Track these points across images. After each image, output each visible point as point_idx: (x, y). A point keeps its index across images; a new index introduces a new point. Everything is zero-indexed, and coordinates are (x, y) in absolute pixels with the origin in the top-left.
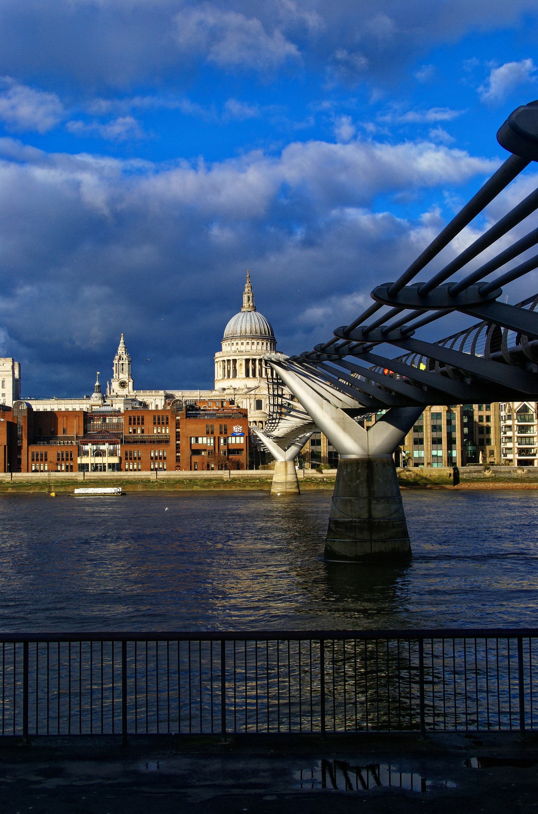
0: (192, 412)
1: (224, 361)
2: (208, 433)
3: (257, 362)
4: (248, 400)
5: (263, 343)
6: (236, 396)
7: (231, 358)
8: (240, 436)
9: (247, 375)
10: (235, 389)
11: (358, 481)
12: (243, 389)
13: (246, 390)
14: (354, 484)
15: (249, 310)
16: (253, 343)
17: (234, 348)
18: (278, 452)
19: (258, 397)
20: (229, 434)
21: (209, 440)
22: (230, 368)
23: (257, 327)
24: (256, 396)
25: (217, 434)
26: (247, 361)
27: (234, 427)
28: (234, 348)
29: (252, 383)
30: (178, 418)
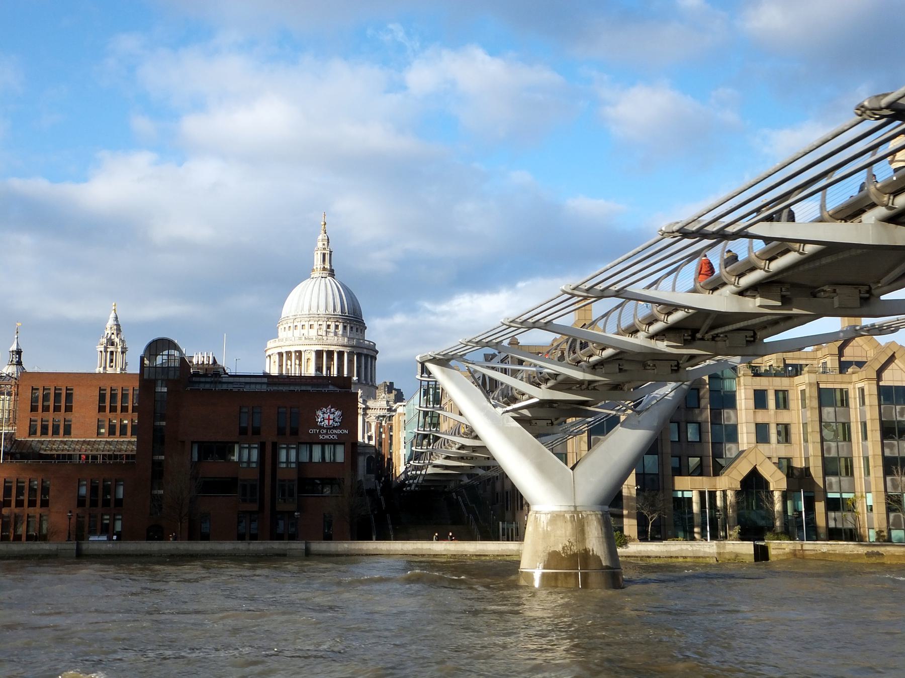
1: (280, 355)
7: (292, 349)
17: (297, 333)
18: (541, 468)
21: (246, 452)
26: (319, 354)
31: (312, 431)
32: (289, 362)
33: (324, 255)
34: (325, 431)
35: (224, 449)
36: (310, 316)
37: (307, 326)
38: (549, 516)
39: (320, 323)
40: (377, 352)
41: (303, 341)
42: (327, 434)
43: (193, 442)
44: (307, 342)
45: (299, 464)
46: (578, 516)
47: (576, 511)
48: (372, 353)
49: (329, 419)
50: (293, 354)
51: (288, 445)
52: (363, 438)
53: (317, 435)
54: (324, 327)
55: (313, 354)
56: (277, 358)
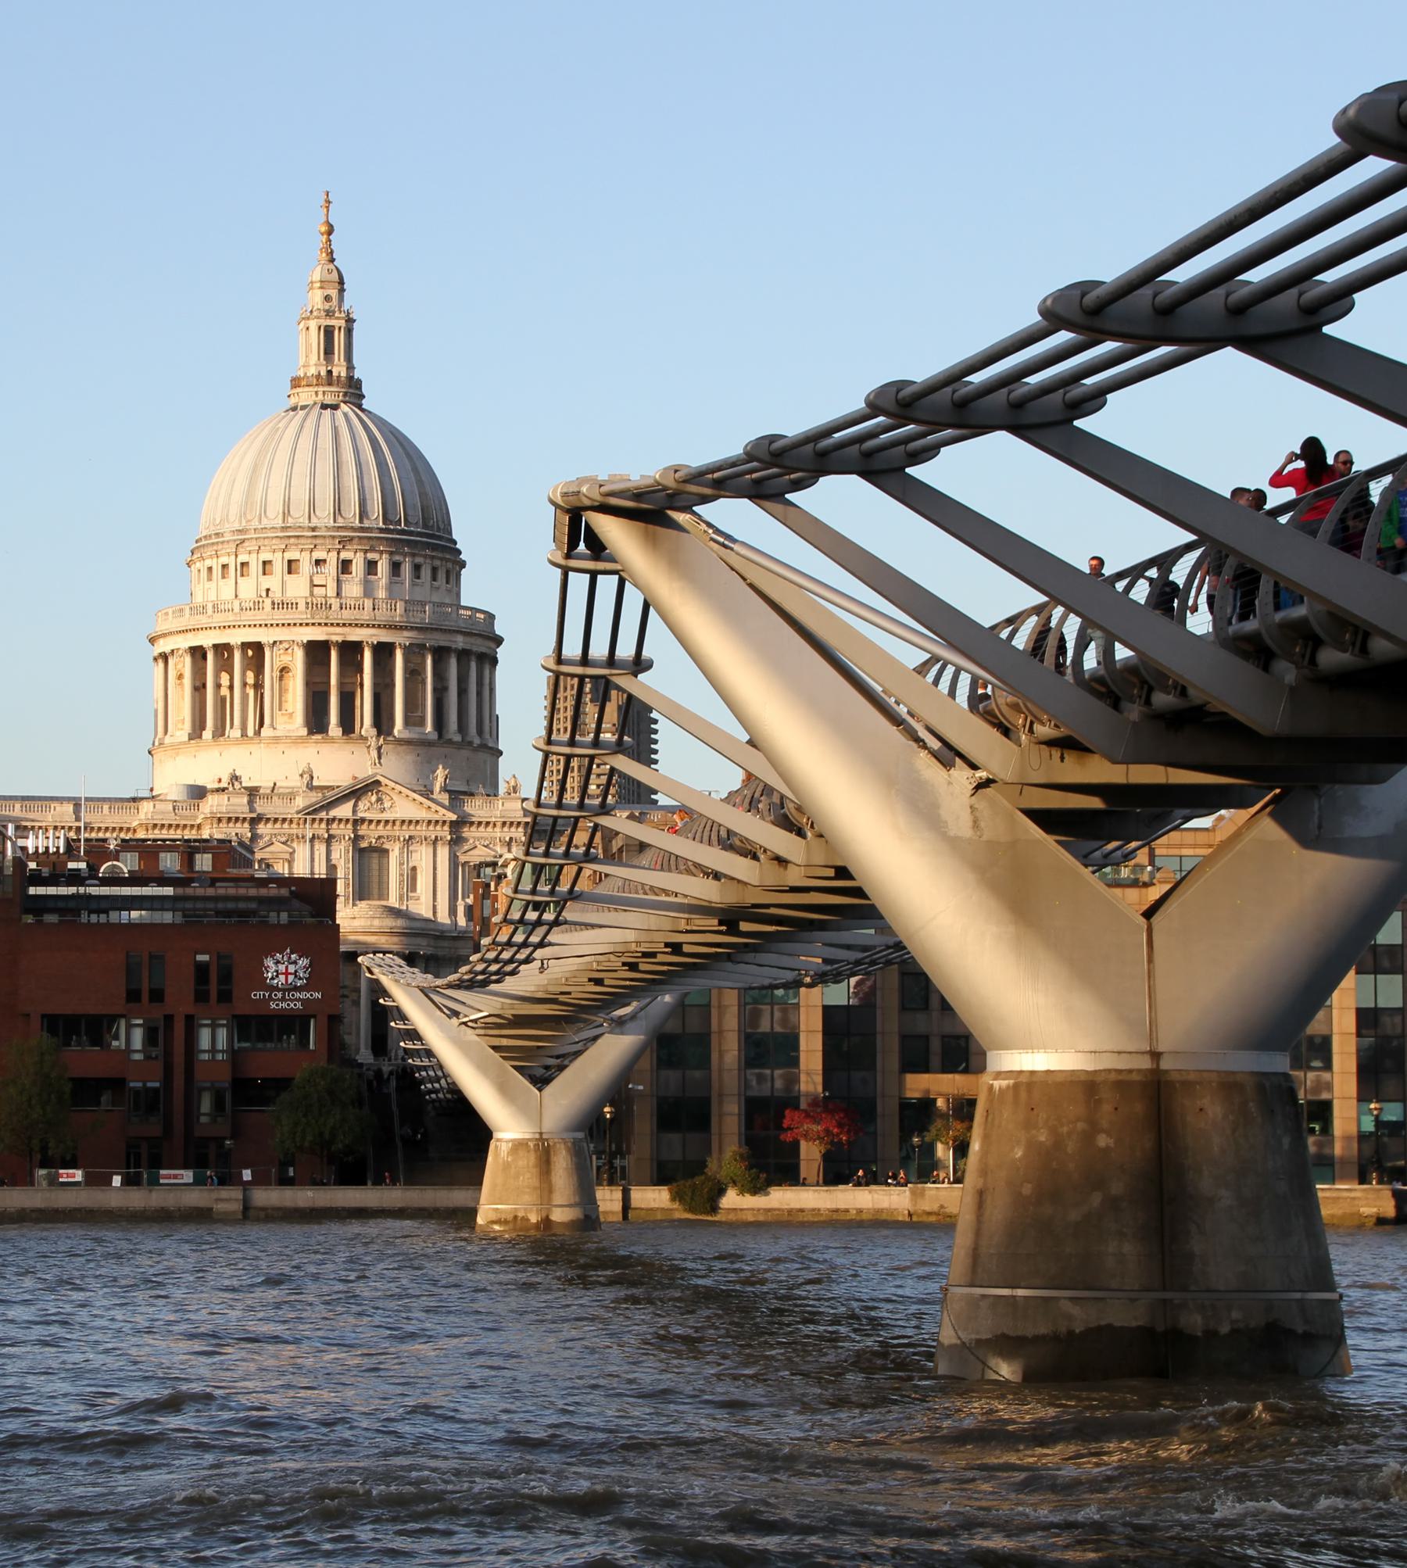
0: (52, 891)
1: (198, 653)
2: (133, 996)
4: (321, 849)
6: (262, 829)
7: (235, 638)
9: (316, 722)
10: (253, 792)
11: (1096, 1199)
12: (291, 796)
13: (315, 797)
14: (1074, 1215)
15: (329, 400)
17: (248, 588)
18: (504, 1089)
25: (180, 998)
26: (316, 652)
28: (248, 588)
29: (338, 762)
31: (257, 995)
32: (225, 679)
33: (329, 332)
34: (280, 995)
35: (97, 1028)
36: (288, 534)
37: (279, 566)
39: (319, 554)
40: (499, 641)
41: (267, 613)
42: (283, 999)
43: (43, 1016)
45: (234, 1054)
47: (541, 1138)
49: (287, 974)
50: (237, 655)
51: (214, 1020)
52: (453, 911)
53: (265, 1002)
54: (331, 568)
55: (299, 654)
56: (186, 664)
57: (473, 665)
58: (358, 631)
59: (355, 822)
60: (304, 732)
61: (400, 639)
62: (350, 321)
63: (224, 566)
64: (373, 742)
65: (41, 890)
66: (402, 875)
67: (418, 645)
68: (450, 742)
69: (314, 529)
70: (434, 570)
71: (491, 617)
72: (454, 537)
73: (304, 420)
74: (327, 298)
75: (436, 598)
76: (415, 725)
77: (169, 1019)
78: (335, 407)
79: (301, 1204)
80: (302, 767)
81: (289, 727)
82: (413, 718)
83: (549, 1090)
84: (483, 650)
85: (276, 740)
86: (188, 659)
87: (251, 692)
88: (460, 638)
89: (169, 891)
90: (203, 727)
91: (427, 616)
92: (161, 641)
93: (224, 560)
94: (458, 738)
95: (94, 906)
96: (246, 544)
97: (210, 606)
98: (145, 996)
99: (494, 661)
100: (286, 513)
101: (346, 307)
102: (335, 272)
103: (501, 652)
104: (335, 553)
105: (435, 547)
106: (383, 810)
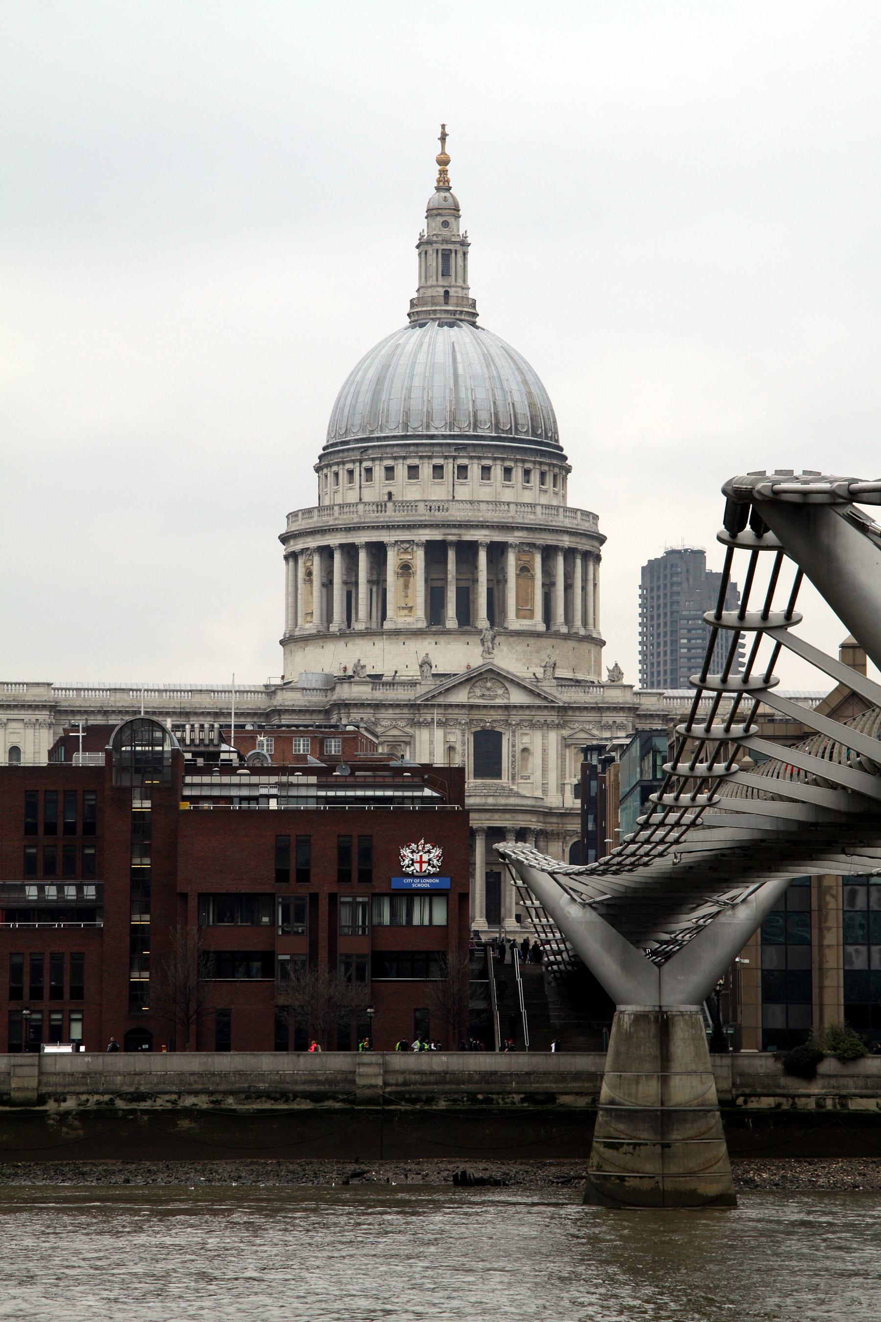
1: (326, 552)
2: (282, 876)
3: (483, 556)
5: (508, 471)
7: (361, 538)
8: (430, 894)
10: (376, 679)
12: (413, 684)
16: (462, 471)
17: (374, 491)
19: (489, 719)
20: (379, 886)
22: (356, 584)
23: (481, 395)
24: (477, 715)
25: (323, 879)
26: (435, 552)
27: (406, 852)
29: (455, 656)
30: (142, 805)
33: (446, 256)
37: (401, 471)
38: (632, 1017)
40: (602, 540)
41: (391, 514)
43: (200, 895)
44: (399, 517)
46: (662, 1016)
48: (584, 545)
50: (363, 556)
55: (420, 554)
56: (316, 562)
57: (579, 562)
58: (473, 532)
59: (472, 707)
60: (422, 624)
61: (511, 538)
62: (464, 244)
63: (351, 472)
64: (489, 635)
65: (197, 779)
66: (514, 756)
67: (529, 544)
68: (557, 635)
69: (432, 437)
70: (543, 474)
71: (596, 517)
72: (561, 444)
73: (424, 336)
74: (445, 224)
75: (544, 500)
76: (525, 618)
77: (314, 897)
78: (451, 325)
79: (436, 1068)
80: (422, 656)
81: (409, 619)
82: (524, 612)
83: (666, 967)
84: (588, 548)
85: (396, 633)
86: (316, 559)
87: (374, 589)
88: (566, 538)
89: (313, 780)
90: (329, 618)
91: (538, 517)
92: (292, 542)
93: (349, 466)
94: (564, 630)
95: (245, 792)
96: (370, 452)
97: (336, 508)
98: (293, 876)
99: (598, 558)
100: (406, 426)
101: (461, 232)
102: (450, 200)
103: (604, 550)
104: (451, 461)
105: (543, 454)
106: (496, 696)
